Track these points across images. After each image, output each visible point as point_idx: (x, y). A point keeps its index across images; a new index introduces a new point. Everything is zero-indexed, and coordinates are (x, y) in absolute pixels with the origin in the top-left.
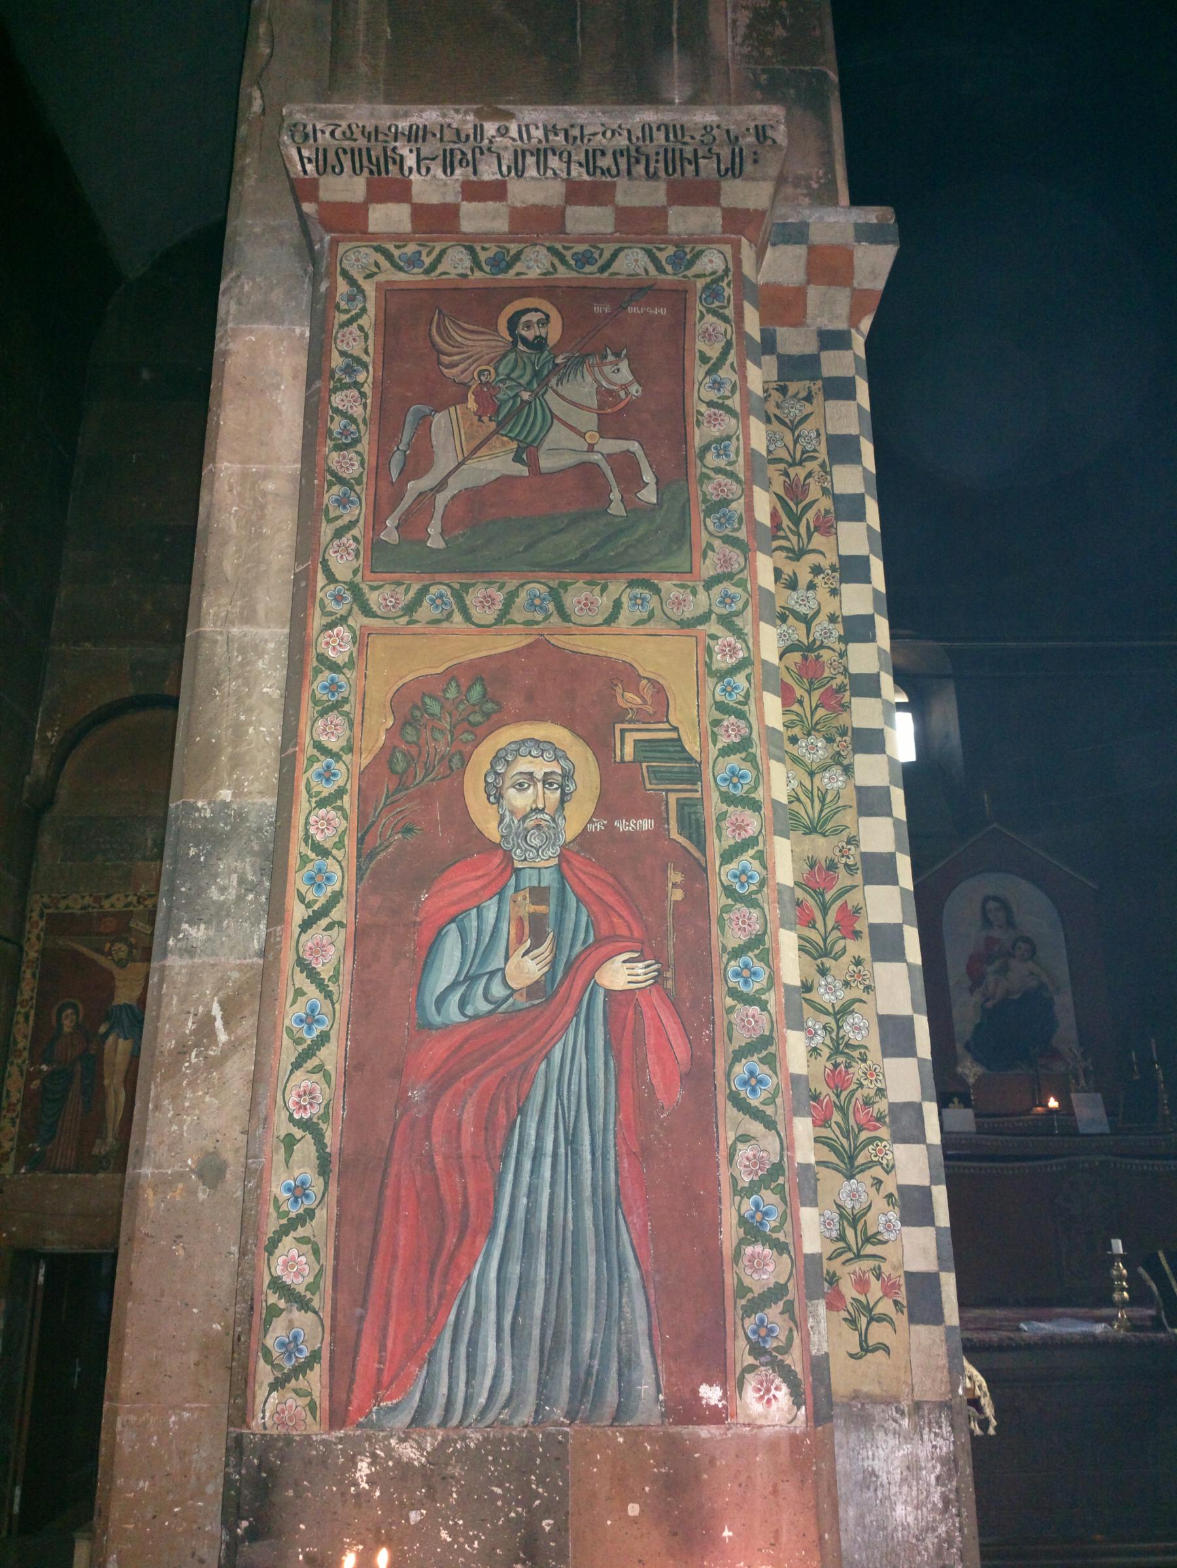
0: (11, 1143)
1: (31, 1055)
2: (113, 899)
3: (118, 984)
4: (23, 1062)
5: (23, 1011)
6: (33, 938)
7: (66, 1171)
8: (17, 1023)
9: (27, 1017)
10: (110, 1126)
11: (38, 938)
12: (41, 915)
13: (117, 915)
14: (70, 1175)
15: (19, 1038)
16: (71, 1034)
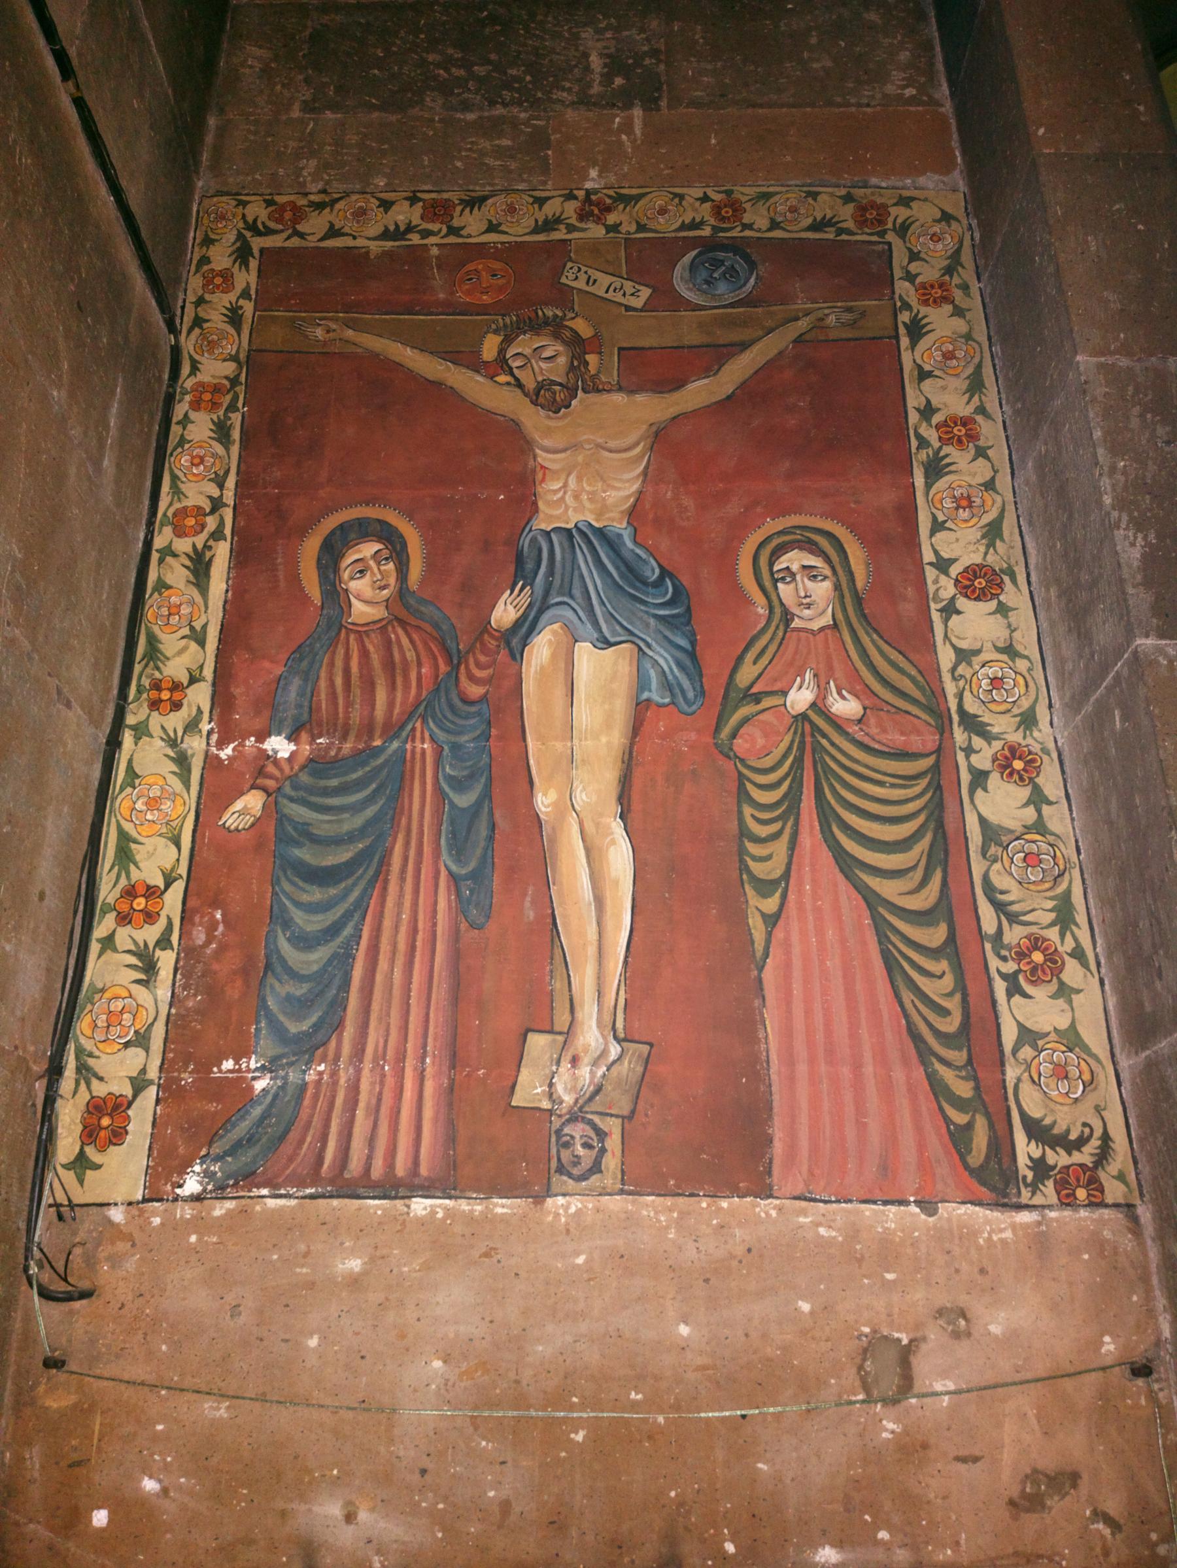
0: (134, 1059)
1: (222, 699)
2: (494, 208)
3: (543, 457)
4: (192, 726)
5: (183, 545)
6: (216, 319)
7: (413, 1187)
8: (162, 586)
9: (200, 567)
10: (584, 980)
11: (234, 317)
12: (242, 254)
13: (513, 253)
14: (420, 1206)
15: (170, 642)
16: (382, 627)
